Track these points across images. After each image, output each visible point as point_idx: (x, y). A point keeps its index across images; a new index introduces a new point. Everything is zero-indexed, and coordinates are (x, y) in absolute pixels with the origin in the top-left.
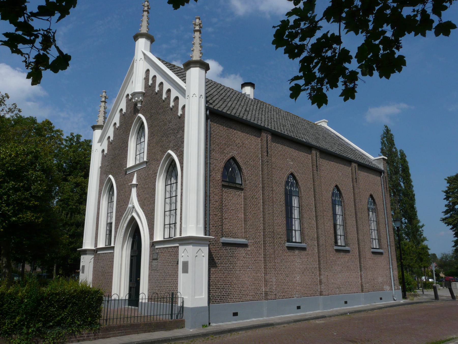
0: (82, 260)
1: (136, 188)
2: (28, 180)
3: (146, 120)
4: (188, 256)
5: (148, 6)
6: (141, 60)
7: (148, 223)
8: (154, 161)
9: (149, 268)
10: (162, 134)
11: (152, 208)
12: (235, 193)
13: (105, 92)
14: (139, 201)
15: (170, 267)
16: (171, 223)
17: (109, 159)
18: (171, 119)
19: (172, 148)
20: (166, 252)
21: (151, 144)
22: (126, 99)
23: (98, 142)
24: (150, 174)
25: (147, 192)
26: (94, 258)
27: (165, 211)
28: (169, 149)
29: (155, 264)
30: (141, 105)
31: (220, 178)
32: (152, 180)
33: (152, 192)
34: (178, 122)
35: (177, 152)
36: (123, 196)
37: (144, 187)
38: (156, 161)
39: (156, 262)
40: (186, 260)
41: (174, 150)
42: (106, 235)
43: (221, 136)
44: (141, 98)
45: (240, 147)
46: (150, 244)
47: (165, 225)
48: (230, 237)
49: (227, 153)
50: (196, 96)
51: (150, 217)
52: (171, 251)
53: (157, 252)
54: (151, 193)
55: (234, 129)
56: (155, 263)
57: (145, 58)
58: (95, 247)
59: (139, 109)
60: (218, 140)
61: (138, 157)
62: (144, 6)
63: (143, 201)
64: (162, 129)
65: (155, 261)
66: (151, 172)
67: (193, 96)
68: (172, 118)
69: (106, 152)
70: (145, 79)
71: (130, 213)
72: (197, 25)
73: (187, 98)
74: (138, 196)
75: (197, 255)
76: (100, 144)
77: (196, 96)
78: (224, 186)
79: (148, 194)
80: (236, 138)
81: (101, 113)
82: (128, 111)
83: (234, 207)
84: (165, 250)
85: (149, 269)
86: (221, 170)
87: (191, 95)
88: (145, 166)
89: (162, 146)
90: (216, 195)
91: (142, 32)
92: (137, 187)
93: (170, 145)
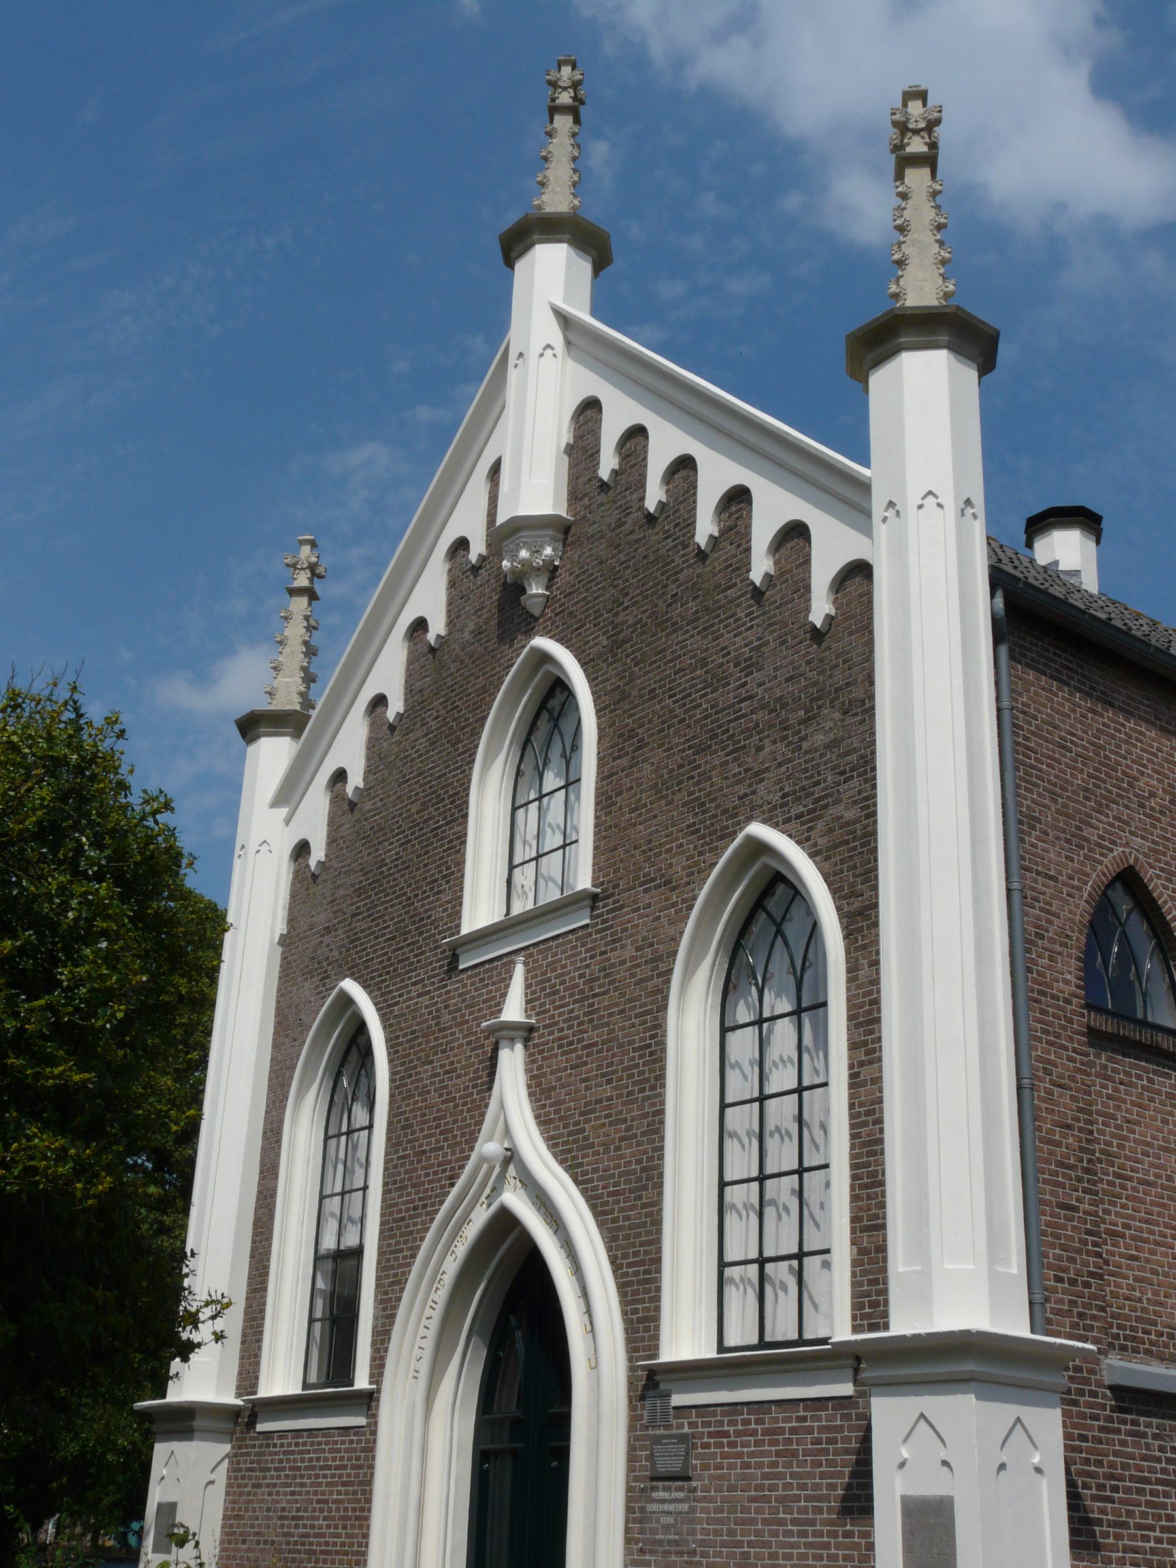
0: (158, 1468)
1: (526, 1047)
2: (46, 926)
3: (584, 665)
4: (945, 1463)
5: (575, 85)
6: (549, 352)
7: (609, 1249)
8: (645, 891)
9: (627, 1530)
10: (694, 737)
11: (639, 1162)
12: (1150, 1081)
13: (313, 544)
14: (543, 1121)
15: (789, 1534)
16: (768, 1253)
17: (342, 892)
18: (757, 649)
19: (775, 808)
20: (754, 1433)
21: (620, 793)
22: (447, 566)
23: (276, 803)
24: (623, 962)
25: (599, 1067)
26: (233, 1458)
27: (728, 1178)
28: (749, 820)
29: (666, 1507)
30: (547, 588)
31: (1078, 986)
32: (631, 1000)
33: (637, 1066)
34: (808, 663)
35: (810, 829)
36: (433, 1097)
37: (580, 1040)
38: (656, 887)
39: (681, 1495)
40: (931, 1487)
41: (789, 820)
42: (311, 1321)
43: (1063, 747)
44: (548, 551)
45: (1161, 812)
46: (631, 1383)
47: (722, 1264)
48: (1147, 1352)
49: (1099, 845)
50: (940, 505)
51: (627, 1218)
52: (793, 1431)
53: (686, 1430)
54: (630, 1077)
55: (1121, 709)
57: (568, 343)
58: (238, 1395)
59: (537, 613)
60: (1048, 765)
61: (525, 877)
62: (554, 85)
63: (577, 1123)
64: (700, 705)
66: (629, 952)
67: (920, 507)
68: (766, 643)
69: (318, 853)
70: (570, 450)
71: (487, 1191)
72: (916, 132)
73: (885, 520)
74: (539, 1090)
75: (1004, 1458)
76: (284, 811)
77: (940, 505)
78: (1096, 1037)
79: (609, 1082)
80: (1138, 761)
81: (287, 650)
82: (461, 631)
83: (1152, 1165)
84: (746, 1422)
85: (629, 1540)
86: (1078, 938)
87: (913, 499)
88: (587, 921)
89: (703, 804)
90: (1060, 1086)
91: (549, 209)
92: (526, 1041)
93: (754, 792)
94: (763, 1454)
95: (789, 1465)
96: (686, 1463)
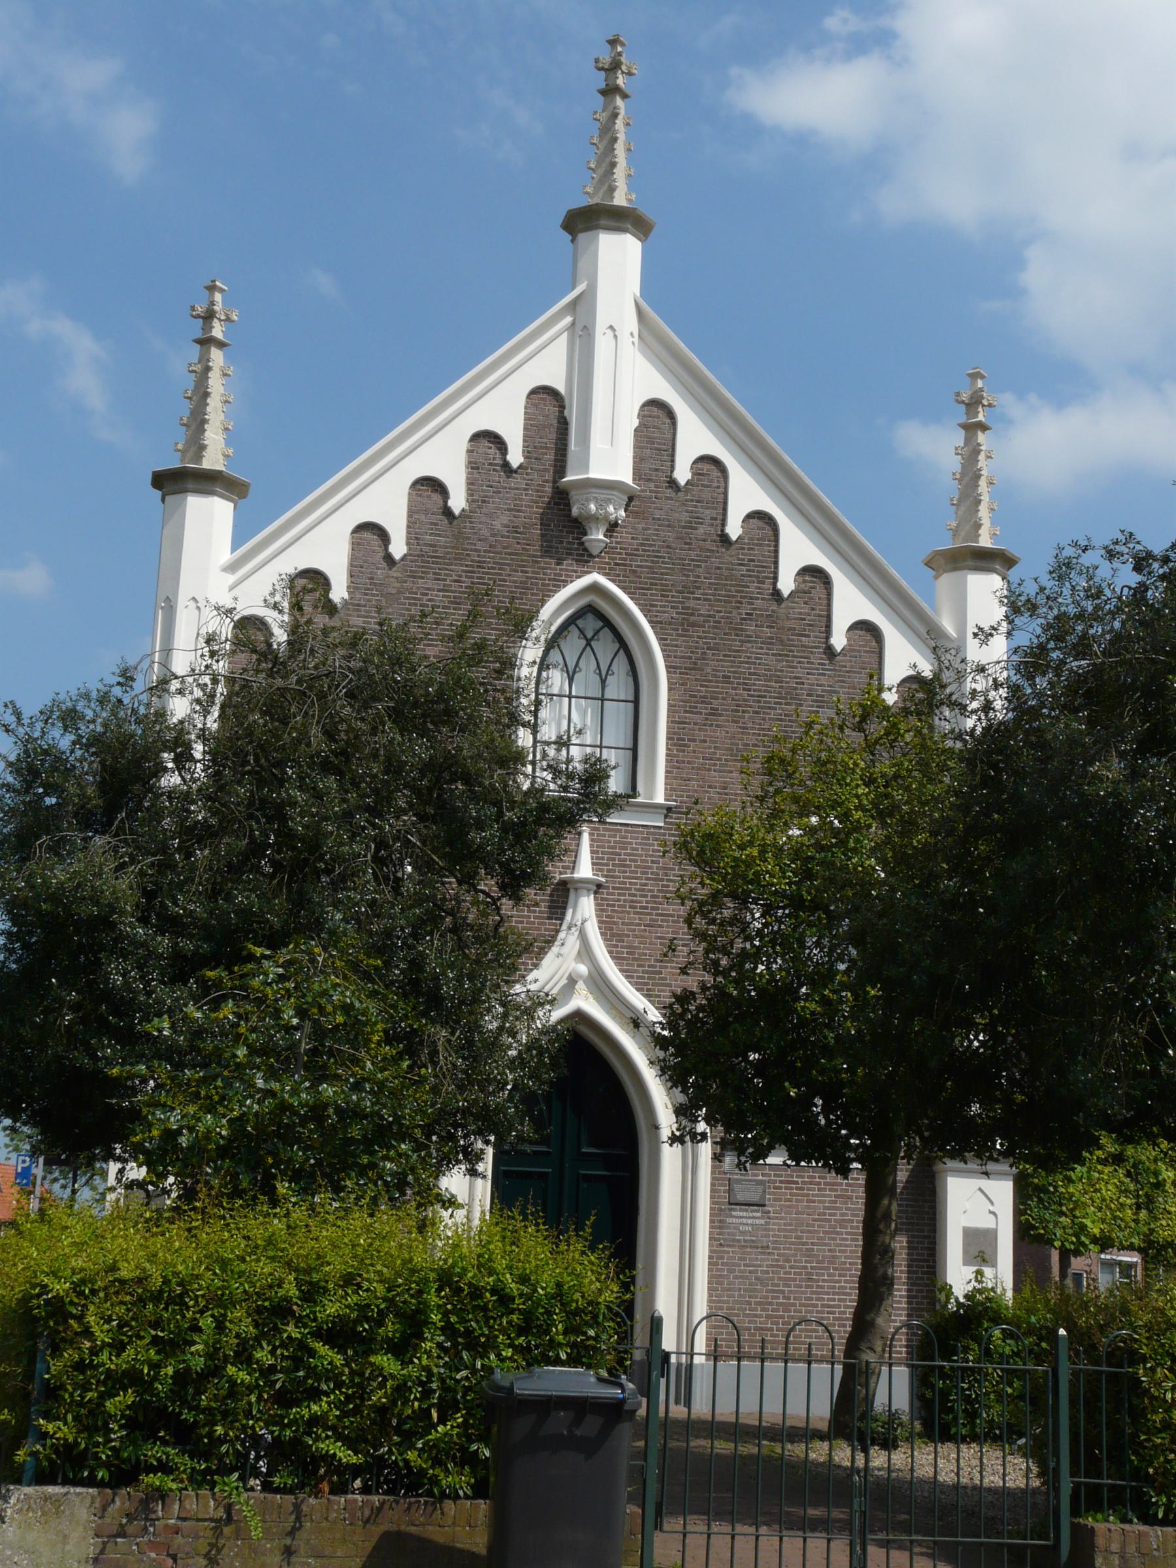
14: (617, 958)
29: (745, 1221)
39: (759, 1214)
56: (754, 1218)
65: (741, 1210)
88: (662, 824)
92: (596, 893)
94: (824, 1196)
95: (846, 1203)
96: (763, 1196)
